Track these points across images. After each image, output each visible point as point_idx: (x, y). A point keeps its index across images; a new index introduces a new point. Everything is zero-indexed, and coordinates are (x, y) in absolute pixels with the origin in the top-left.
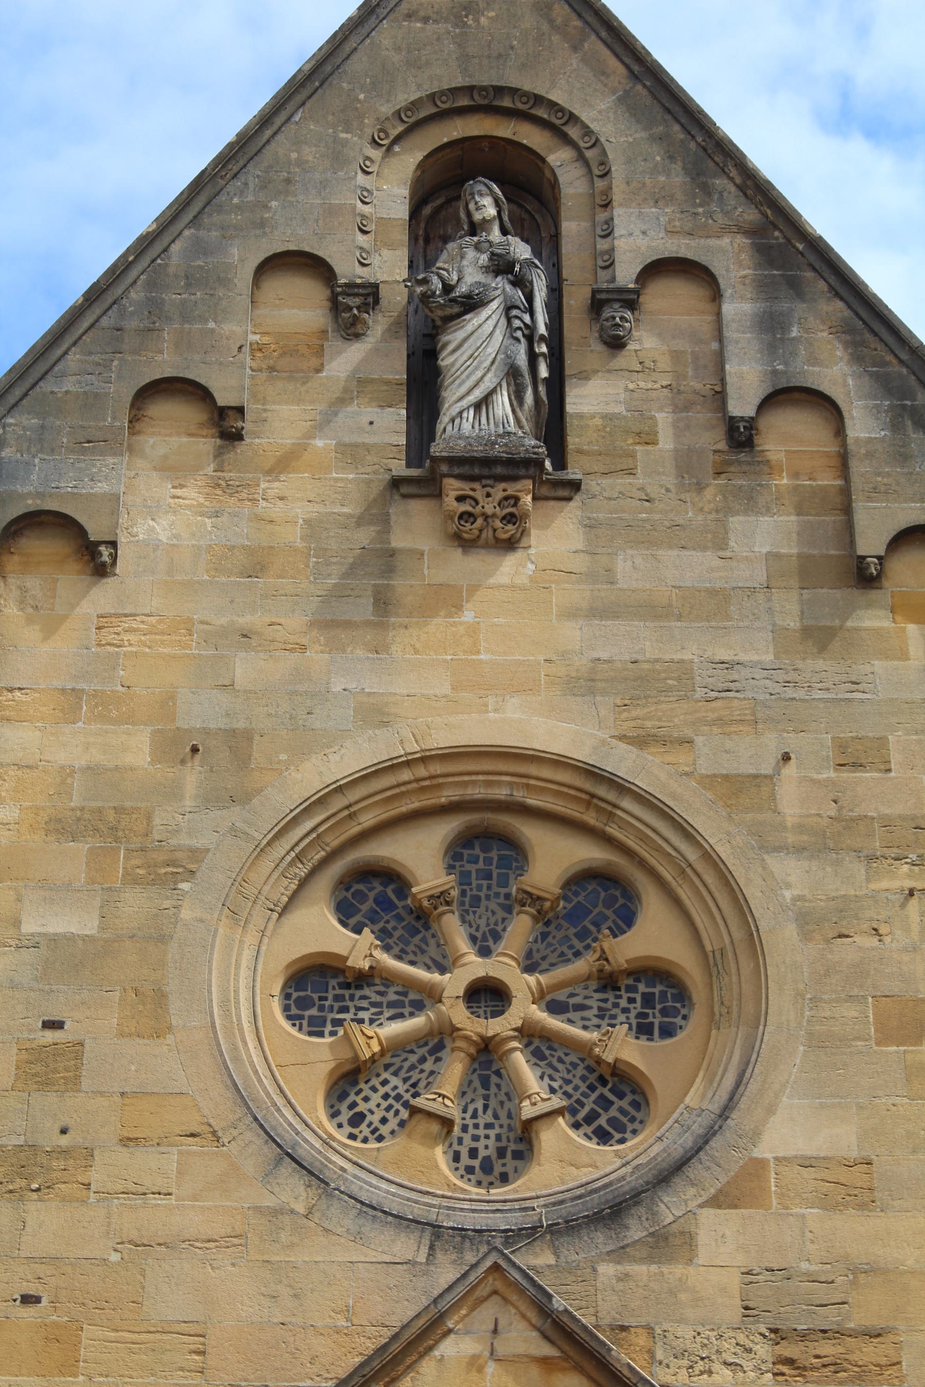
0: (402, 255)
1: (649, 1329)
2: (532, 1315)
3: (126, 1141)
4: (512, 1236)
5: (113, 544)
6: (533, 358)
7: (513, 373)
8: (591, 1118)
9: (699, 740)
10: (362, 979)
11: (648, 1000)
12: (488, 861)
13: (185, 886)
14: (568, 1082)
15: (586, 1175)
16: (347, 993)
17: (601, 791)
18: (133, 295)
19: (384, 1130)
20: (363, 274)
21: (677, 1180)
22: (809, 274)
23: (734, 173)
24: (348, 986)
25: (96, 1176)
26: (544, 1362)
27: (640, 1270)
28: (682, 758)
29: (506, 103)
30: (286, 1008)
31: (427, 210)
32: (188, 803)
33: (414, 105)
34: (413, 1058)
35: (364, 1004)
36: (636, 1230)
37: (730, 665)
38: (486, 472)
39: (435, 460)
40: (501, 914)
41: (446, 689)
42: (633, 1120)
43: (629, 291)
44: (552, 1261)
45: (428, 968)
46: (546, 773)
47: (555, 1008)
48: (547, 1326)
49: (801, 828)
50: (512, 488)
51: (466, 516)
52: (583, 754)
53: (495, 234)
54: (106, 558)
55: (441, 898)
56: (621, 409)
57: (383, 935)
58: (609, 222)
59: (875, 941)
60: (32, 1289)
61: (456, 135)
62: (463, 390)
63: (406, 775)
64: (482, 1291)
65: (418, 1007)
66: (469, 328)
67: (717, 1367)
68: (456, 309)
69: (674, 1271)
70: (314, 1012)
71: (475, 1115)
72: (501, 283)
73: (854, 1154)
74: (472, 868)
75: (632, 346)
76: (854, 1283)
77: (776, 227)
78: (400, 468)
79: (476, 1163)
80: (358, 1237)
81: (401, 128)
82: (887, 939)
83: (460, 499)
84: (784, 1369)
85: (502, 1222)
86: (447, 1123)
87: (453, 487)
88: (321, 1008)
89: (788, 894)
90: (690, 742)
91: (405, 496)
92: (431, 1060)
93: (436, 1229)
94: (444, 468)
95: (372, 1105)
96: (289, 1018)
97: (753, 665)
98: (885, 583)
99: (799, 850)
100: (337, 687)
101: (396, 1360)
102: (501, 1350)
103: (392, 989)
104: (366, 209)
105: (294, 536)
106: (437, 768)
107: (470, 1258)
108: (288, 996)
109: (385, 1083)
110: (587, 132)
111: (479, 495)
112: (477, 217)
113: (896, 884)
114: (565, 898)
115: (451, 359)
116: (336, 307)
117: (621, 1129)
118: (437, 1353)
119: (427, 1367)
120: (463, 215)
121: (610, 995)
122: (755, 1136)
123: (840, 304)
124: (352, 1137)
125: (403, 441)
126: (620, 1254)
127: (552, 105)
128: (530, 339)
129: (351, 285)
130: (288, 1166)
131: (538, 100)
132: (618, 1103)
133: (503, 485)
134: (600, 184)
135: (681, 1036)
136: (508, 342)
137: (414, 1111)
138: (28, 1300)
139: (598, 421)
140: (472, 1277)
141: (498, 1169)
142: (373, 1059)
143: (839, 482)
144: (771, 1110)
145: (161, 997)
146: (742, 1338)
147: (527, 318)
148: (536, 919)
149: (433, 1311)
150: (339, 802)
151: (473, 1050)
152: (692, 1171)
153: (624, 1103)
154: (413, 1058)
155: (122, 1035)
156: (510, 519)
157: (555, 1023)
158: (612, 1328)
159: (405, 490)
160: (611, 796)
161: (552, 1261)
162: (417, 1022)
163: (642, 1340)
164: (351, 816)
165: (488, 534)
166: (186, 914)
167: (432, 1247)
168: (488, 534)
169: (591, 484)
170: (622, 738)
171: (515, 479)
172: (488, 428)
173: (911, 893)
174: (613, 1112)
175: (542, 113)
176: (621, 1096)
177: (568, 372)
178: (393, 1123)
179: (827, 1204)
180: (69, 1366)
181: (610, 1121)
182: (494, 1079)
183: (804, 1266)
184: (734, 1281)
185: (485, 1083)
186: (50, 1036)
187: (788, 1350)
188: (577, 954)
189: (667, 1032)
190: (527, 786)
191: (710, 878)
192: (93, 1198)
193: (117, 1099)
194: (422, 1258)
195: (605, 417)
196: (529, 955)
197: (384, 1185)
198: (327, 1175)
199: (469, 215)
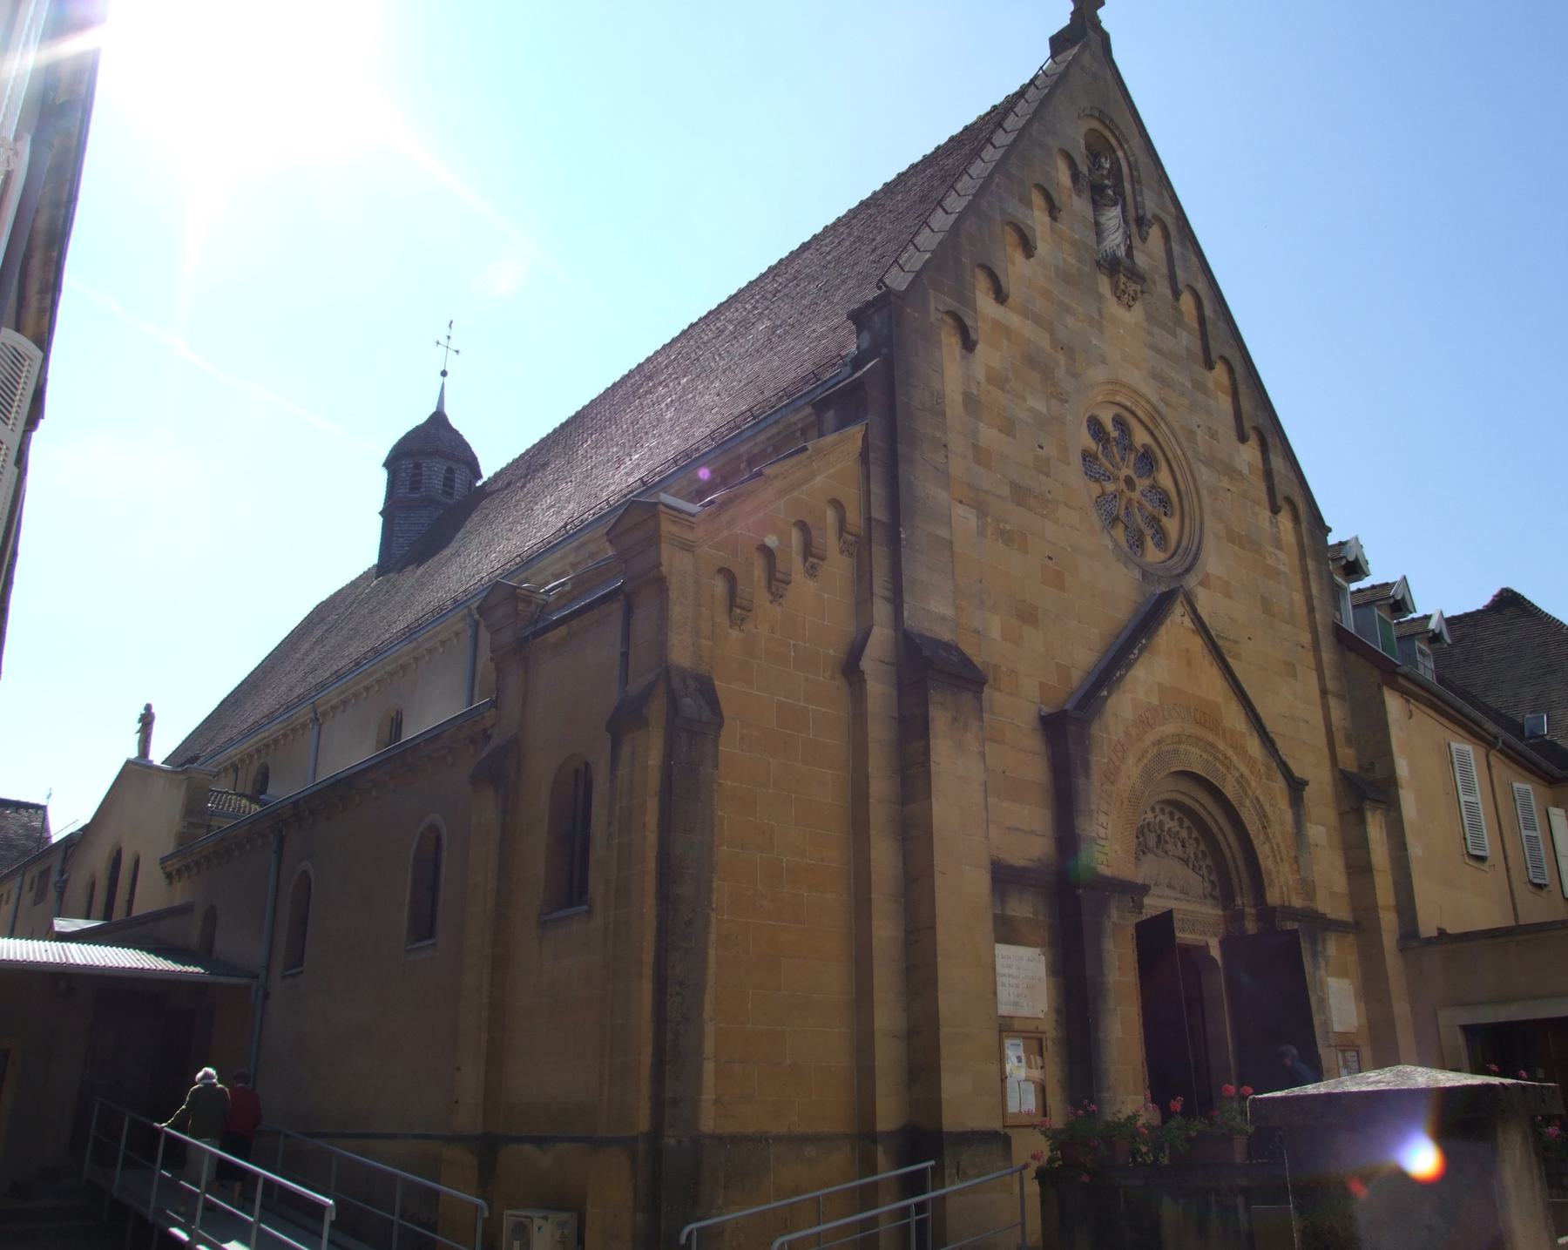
16: (1092, 465)
55: (1114, 439)
58: (1141, 190)
99: (1204, 463)
100: (1094, 342)
115: (1108, 222)
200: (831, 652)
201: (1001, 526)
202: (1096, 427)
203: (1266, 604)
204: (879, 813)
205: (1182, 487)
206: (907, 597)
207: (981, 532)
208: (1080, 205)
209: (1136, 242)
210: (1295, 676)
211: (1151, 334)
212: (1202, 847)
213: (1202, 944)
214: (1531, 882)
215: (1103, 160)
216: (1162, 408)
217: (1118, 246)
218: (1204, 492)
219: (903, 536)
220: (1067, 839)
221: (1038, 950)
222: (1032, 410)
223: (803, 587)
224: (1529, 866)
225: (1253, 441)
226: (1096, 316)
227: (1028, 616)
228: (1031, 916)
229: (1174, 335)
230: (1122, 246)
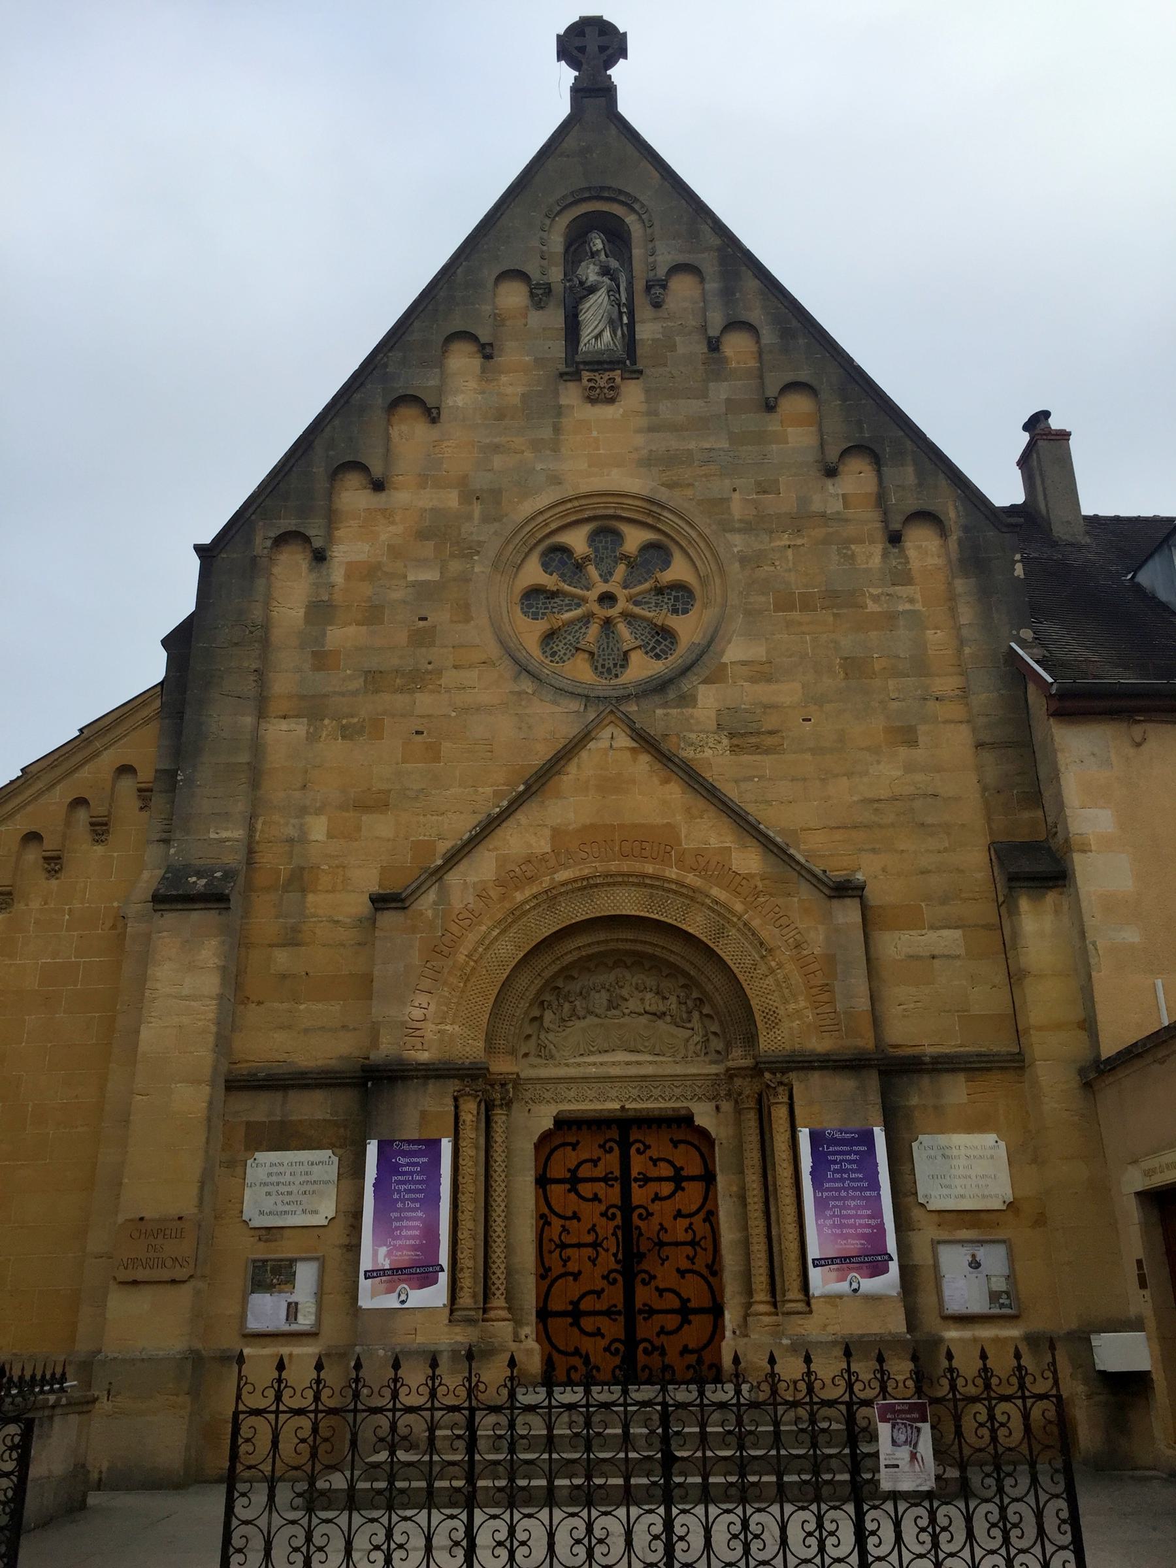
0: (561, 268)
1: (678, 735)
2: (628, 731)
3: (455, 667)
4: (619, 699)
5: (438, 408)
6: (620, 313)
7: (611, 322)
8: (654, 648)
9: (697, 484)
10: (553, 595)
11: (676, 599)
12: (606, 542)
13: (476, 558)
14: (642, 635)
15: (650, 673)
16: (547, 601)
17: (654, 508)
18: (441, 294)
19: (565, 658)
20: (545, 279)
21: (689, 673)
22: (744, 268)
23: (709, 222)
24: (548, 598)
25: (443, 681)
26: (633, 749)
27: (674, 711)
28: (689, 492)
29: (606, 194)
30: (522, 609)
31: (572, 249)
32: (476, 522)
33: (564, 197)
34: (577, 628)
35: (555, 605)
36: (672, 695)
37: (711, 450)
38: (600, 367)
39: (578, 363)
40: (613, 564)
41: (584, 466)
42: (671, 649)
43: (663, 280)
44: (636, 709)
45: (582, 589)
46: (630, 501)
47: (636, 603)
48: (634, 735)
49: (740, 521)
50: (612, 374)
51: (592, 388)
52: (645, 492)
53: (603, 256)
54: (435, 415)
55: (587, 558)
56: (660, 336)
57: (562, 576)
58: (654, 248)
59: (772, 568)
60: (420, 729)
61: (583, 211)
62: (589, 331)
63: (569, 505)
64: (606, 722)
65: (579, 605)
66: (592, 301)
67: (706, 749)
68: (585, 293)
69: (689, 711)
70: (534, 610)
71: (603, 650)
72: (606, 279)
73: (764, 659)
74: (600, 545)
75: (665, 307)
76: (764, 713)
77: (728, 246)
78: (562, 368)
79: (605, 670)
80: (555, 702)
81: (559, 208)
82: (778, 568)
83: (589, 380)
84: (735, 749)
85: (615, 694)
86: (592, 654)
87: (586, 375)
88: (537, 608)
89: (736, 550)
90: (693, 485)
91: (566, 381)
92: (584, 628)
93: (587, 697)
94: (582, 367)
95: (560, 648)
96: (523, 613)
97: (720, 449)
98: (778, 409)
99: (739, 531)
100: (539, 467)
101: (570, 751)
102: (615, 745)
103: (566, 599)
104: (545, 248)
105: (516, 401)
106: (583, 502)
107: (602, 708)
108: (523, 604)
109: (565, 638)
110: (643, 206)
111: (597, 378)
112: (594, 249)
113: (783, 543)
114: (640, 556)
116: (532, 295)
117: (665, 653)
118: (588, 747)
119: (584, 754)
120: (588, 249)
121: (660, 597)
122: (723, 653)
123: (757, 281)
124: (552, 661)
125: (563, 355)
126: (665, 705)
127: (627, 194)
128: (619, 305)
129: (538, 284)
130: (524, 674)
131: (620, 192)
132: (664, 643)
133: (608, 373)
134: (649, 231)
135: (691, 613)
136: (609, 307)
137: (577, 649)
138: (417, 733)
139: (650, 342)
140: (602, 716)
141: (614, 672)
142: (559, 628)
143: (758, 365)
144: (729, 642)
145: (467, 606)
146: (717, 738)
147: (617, 296)
148: (627, 566)
149: (585, 730)
150: (541, 519)
151: (602, 623)
152: (694, 669)
153: (667, 643)
154: (577, 628)
155: (452, 621)
156: (612, 388)
157: (637, 610)
158: (662, 735)
159: (565, 378)
160: (659, 511)
161: (636, 709)
162: (579, 612)
163: (675, 739)
164: (546, 524)
165: (602, 396)
166: (477, 570)
167: (586, 705)
168: (602, 396)
169: (647, 371)
170: (662, 485)
171: (614, 370)
172: (600, 345)
173: (789, 547)
174: (662, 646)
175: (622, 198)
176: (665, 640)
177: (636, 319)
178: (569, 655)
179: (753, 680)
180: (437, 758)
181: (661, 650)
182: (611, 635)
183: (743, 706)
184: (713, 714)
185: (607, 636)
186: (422, 623)
187: (735, 741)
188: (646, 580)
189: (685, 612)
190: (622, 508)
191: (702, 545)
192: (443, 691)
193: (451, 649)
194: (582, 709)
195: (653, 340)
196: (625, 581)
197: (565, 681)
198: (542, 677)
199: (591, 248)
201: (344, 722)
203: (854, 667)
209: (644, 311)
210: (913, 743)
211: (649, 413)
216: (663, 495)
217: (598, 336)
222: (414, 584)
226: (546, 433)
228: (328, 1117)
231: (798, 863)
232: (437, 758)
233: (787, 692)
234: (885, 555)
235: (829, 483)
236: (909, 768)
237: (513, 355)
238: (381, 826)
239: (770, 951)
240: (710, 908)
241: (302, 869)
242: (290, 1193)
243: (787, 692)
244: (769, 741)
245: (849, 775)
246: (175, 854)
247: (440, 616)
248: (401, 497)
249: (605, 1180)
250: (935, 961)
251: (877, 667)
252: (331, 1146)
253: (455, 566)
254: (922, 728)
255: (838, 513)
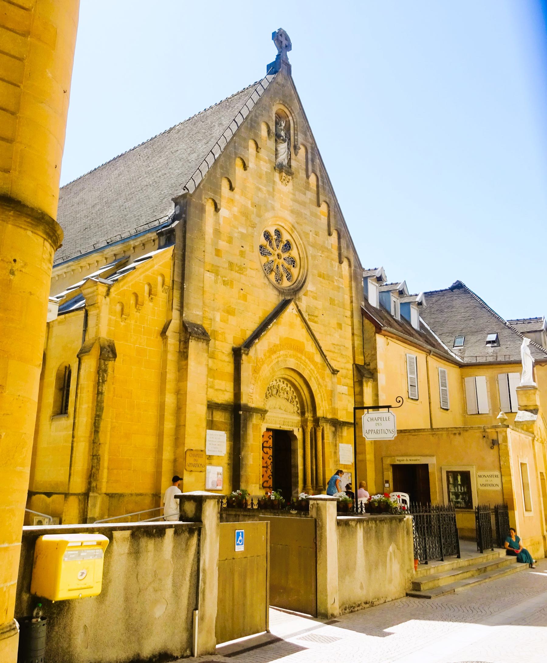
58: (297, 134)
100: (269, 201)
138: (242, 289)
145: (253, 246)
166: (255, 234)
200: (157, 328)
202: (267, 236)
203: (332, 301)
204: (170, 386)
205: (301, 256)
206: (185, 309)
207: (216, 282)
208: (271, 144)
209: (293, 156)
210: (341, 329)
211: (294, 194)
212: (295, 394)
213: (291, 430)
214: (441, 408)
215: (282, 122)
218: (310, 258)
219: (185, 287)
220: (237, 394)
221: (224, 432)
223: (148, 305)
224: (441, 401)
225: (335, 234)
226: (271, 190)
227: (230, 311)
228: (223, 421)
229: (305, 194)
230: (286, 160)
231: (328, 362)
232: (246, 301)
233: (319, 304)
234: (338, 267)
235: (329, 237)
236: (340, 337)
237: (263, 153)
238: (233, 320)
239: (321, 386)
240: (309, 370)
241: (214, 331)
242: (215, 445)
243: (319, 304)
244: (316, 319)
245: (330, 335)
246: (185, 316)
247: (247, 248)
248: (237, 195)
249: (269, 447)
250: (343, 395)
251: (336, 303)
252: (224, 430)
253: (250, 229)
254: (343, 325)
255: (330, 249)
